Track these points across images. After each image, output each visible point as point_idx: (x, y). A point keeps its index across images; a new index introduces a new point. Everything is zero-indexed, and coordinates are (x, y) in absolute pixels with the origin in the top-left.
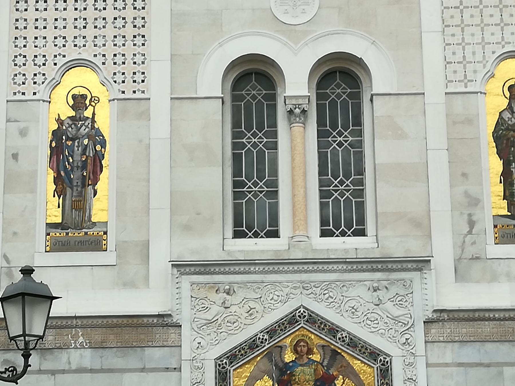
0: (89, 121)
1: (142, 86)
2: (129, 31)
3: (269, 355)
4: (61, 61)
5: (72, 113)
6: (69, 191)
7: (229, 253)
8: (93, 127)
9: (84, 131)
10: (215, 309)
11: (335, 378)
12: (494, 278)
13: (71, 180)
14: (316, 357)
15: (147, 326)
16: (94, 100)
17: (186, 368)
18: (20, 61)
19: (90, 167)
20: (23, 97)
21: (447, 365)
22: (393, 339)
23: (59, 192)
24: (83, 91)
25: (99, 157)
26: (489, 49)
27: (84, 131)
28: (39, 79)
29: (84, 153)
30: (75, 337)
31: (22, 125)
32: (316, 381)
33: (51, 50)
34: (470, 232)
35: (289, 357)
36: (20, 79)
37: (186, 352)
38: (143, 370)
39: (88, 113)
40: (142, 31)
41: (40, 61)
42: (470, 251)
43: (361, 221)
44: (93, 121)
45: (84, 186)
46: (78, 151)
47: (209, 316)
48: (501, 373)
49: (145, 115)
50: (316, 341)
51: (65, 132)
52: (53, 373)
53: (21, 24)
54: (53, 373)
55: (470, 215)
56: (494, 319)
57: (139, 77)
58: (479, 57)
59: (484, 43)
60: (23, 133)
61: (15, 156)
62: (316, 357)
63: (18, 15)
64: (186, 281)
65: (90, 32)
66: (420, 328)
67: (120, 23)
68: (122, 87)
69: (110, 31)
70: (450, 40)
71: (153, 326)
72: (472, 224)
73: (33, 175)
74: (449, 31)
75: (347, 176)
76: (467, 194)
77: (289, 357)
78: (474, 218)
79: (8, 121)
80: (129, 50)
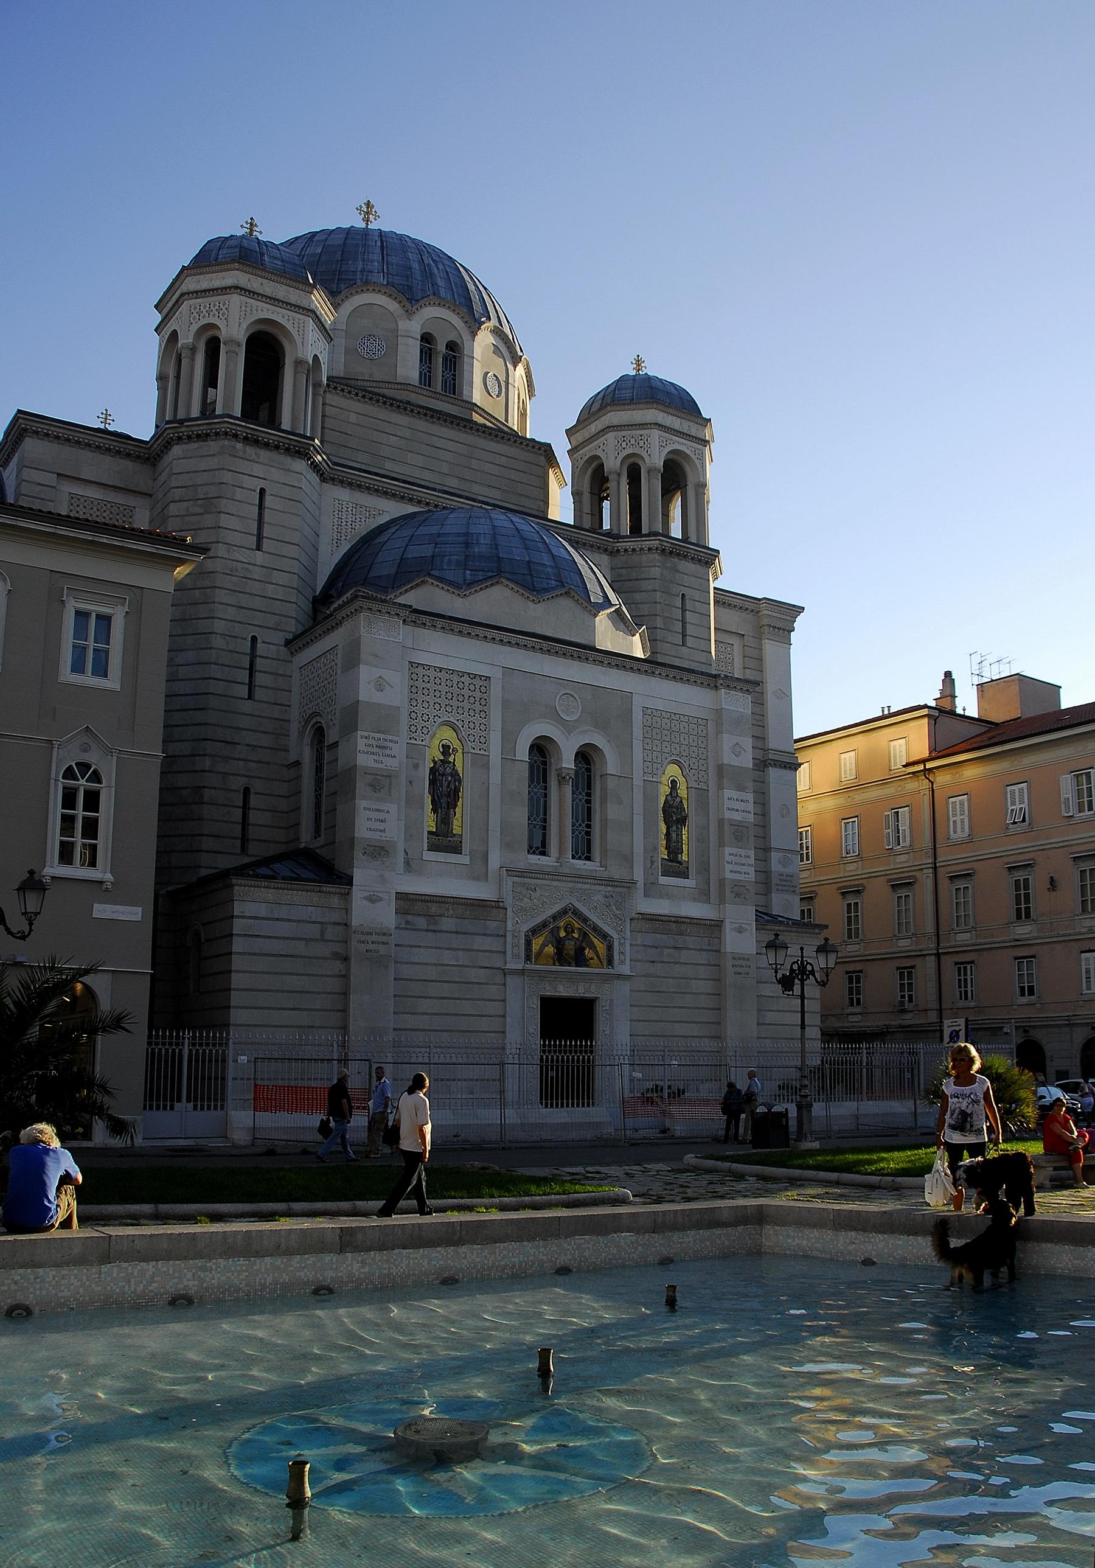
3: (552, 931)
6: (440, 810)
7: (531, 864)
8: (454, 769)
9: (448, 770)
11: (585, 949)
12: (661, 897)
13: (441, 804)
14: (576, 935)
15: (486, 906)
16: (455, 750)
20: (415, 742)
21: (638, 945)
22: (614, 928)
23: (434, 810)
25: (457, 791)
27: (448, 770)
28: (425, 730)
29: (448, 786)
30: (448, 909)
32: (576, 949)
35: (562, 934)
37: (509, 923)
38: (484, 935)
39: (451, 759)
41: (425, 718)
43: (589, 851)
44: (454, 765)
45: (448, 808)
46: (445, 784)
49: (486, 766)
50: (577, 925)
51: (437, 770)
52: (435, 931)
53: (414, 690)
54: (435, 931)
61: (411, 782)
62: (576, 935)
64: (510, 881)
65: (455, 703)
67: (472, 700)
71: (492, 907)
72: (652, 863)
73: (422, 797)
75: (583, 821)
77: (562, 934)
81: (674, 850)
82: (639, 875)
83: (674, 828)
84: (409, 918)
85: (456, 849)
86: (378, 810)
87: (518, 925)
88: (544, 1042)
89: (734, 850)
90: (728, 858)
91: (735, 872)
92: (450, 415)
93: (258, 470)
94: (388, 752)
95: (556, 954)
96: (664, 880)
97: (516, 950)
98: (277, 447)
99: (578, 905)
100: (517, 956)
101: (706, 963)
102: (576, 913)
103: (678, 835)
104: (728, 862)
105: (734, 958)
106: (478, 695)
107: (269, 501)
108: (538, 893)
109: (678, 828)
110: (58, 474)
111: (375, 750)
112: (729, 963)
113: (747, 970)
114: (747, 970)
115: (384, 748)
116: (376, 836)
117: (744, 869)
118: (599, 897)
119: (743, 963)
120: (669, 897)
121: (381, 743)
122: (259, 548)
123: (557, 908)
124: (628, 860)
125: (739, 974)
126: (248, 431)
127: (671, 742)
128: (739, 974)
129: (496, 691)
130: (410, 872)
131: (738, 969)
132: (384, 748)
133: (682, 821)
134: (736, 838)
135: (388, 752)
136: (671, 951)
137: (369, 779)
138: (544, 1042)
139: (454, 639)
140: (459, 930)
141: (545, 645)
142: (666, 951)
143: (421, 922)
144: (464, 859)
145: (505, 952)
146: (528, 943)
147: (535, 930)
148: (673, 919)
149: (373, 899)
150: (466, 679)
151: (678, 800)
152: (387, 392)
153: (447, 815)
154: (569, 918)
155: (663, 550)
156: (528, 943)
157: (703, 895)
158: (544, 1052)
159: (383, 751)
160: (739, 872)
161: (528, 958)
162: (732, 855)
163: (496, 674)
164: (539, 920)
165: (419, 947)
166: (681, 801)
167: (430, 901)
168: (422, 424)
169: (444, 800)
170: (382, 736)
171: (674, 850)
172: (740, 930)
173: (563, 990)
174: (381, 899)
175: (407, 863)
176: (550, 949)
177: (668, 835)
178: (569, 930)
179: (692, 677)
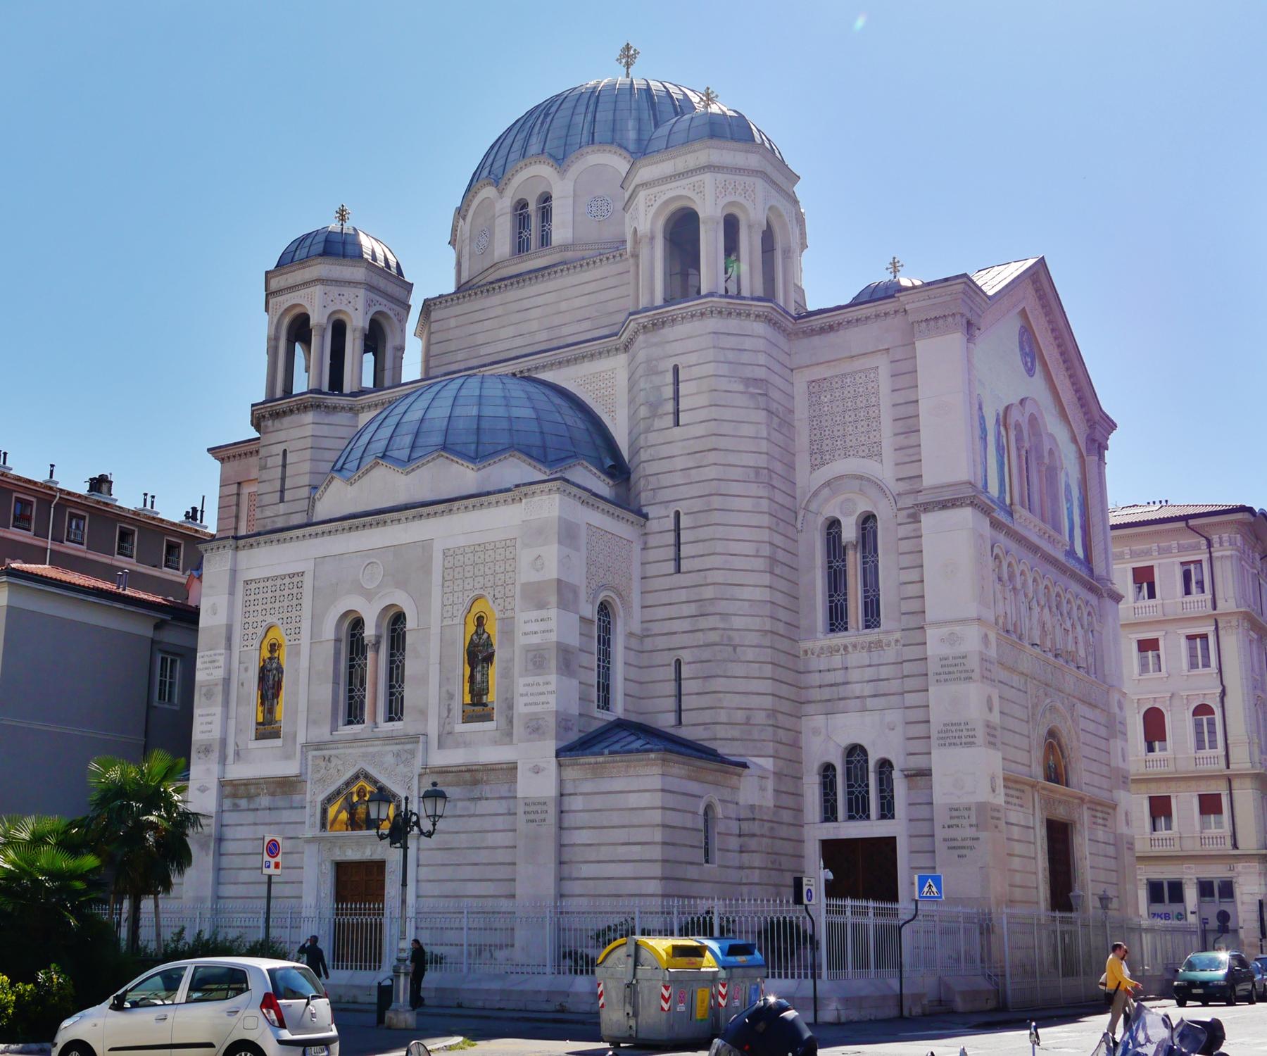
0: (276, 660)
1: (297, 636)
2: (295, 602)
3: (346, 799)
4: (264, 624)
5: (269, 655)
9: (274, 665)
10: (323, 771)
12: (457, 745)
17: (308, 806)
18: (247, 626)
19: (276, 688)
23: (262, 704)
24: (274, 641)
25: (280, 681)
26: (466, 593)
27: (274, 665)
30: (263, 789)
31: (245, 665)
33: (260, 618)
34: (448, 717)
35: (355, 799)
36: (246, 637)
37: (308, 797)
38: (292, 808)
39: (276, 655)
40: (300, 602)
42: (448, 728)
45: (273, 699)
46: (271, 678)
47: (319, 776)
48: (455, 806)
49: (298, 654)
55: (449, 705)
56: (452, 772)
57: (297, 631)
58: (460, 600)
59: (464, 590)
60: (246, 670)
61: (242, 684)
63: (246, 598)
65: (277, 605)
66: (416, 778)
68: (289, 637)
69: (286, 604)
70: (447, 590)
72: (449, 711)
74: (447, 584)
76: (448, 692)
78: (451, 707)
79: (240, 663)
80: (294, 613)
81: (478, 693)
82: (433, 729)
83: (479, 668)
84: (237, 801)
85: (276, 735)
86: (208, 715)
87: (314, 794)
88: (338, 905)
89: (530, 680)
90: (522, 690)
91: (531, 704)
92: (531, 272)
93: (282, 436)
94: (217, 664)
95: (349, 819)
96: (461, 728)
97: (312, 819)
98: (291, 411)
99: (373, 772)
100: (313, 825)
101: (506, 811)
102: (367, 777)
103: (483, 675)
104: (522, 695)
105: (526, 804)
106: (295, 591)
107: (291, 458)
108: (334, 761)
109: (483, 667)
110: (239, 483)
111: (208, 665)
112: (520, 810)
113: (543, 816)
114: (543, 816)
115: (214, 661)
116: (205, 736)
117: (542, 698)
118: (390, 759)
119: (539, 808)
120: (466, 745)
121: (211, 659)
122: (282, 500)
123: (348, 775)
124: (423, 713)
125: (533, 821)
126: (269, 409)
127: (474, 577)
128: (533, 821)
129: (308, 582)
130: (238, 760)
131: (532, 817)
132: (214, 661)
133: (489, 659)
134: (535, 664)
135: (217, 664)
136: (468, 803)
137: (204, 690)
138: (338, 905)
139: (276, 548)
140: (272, 806)
141: (346, 523)
142: (460, 804)
143: (243, 803)
144: (278, 742)
145: (304, 823)
146: (324, 812)
147: (330, 799)
148: (464, 768)
149: (203, 789)
150: (287, 580)
151: (485, 636)
152: (490, 279)
153: (272, 705)
154: (362, 783)
155: (644, 327)
156: (324, 812)
157: (507, 735)
158: (337, 915)
159: (213, 664)
160: (536, 704)
161: (323, 826)
162: (528, 685)
163: (307, 567)
164: (332, 788)
165: (241, 825)
166: (489, 637)
167: (249, 784)
168: (512, 294)
169: (270, 693)
170: (212, 652)
171: (478, 693)
172: (537, 770)
173: (352, 855)
174: (208, 789)
175: (237, 754)
176: (344, 816)
177: (472, 677)
178: (361, 792)
179: (492, 498)
